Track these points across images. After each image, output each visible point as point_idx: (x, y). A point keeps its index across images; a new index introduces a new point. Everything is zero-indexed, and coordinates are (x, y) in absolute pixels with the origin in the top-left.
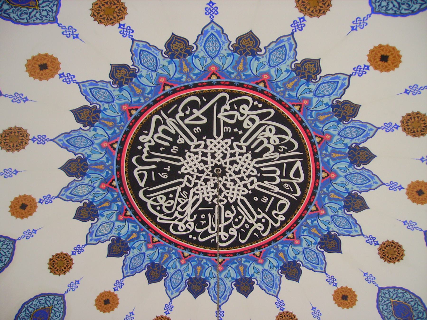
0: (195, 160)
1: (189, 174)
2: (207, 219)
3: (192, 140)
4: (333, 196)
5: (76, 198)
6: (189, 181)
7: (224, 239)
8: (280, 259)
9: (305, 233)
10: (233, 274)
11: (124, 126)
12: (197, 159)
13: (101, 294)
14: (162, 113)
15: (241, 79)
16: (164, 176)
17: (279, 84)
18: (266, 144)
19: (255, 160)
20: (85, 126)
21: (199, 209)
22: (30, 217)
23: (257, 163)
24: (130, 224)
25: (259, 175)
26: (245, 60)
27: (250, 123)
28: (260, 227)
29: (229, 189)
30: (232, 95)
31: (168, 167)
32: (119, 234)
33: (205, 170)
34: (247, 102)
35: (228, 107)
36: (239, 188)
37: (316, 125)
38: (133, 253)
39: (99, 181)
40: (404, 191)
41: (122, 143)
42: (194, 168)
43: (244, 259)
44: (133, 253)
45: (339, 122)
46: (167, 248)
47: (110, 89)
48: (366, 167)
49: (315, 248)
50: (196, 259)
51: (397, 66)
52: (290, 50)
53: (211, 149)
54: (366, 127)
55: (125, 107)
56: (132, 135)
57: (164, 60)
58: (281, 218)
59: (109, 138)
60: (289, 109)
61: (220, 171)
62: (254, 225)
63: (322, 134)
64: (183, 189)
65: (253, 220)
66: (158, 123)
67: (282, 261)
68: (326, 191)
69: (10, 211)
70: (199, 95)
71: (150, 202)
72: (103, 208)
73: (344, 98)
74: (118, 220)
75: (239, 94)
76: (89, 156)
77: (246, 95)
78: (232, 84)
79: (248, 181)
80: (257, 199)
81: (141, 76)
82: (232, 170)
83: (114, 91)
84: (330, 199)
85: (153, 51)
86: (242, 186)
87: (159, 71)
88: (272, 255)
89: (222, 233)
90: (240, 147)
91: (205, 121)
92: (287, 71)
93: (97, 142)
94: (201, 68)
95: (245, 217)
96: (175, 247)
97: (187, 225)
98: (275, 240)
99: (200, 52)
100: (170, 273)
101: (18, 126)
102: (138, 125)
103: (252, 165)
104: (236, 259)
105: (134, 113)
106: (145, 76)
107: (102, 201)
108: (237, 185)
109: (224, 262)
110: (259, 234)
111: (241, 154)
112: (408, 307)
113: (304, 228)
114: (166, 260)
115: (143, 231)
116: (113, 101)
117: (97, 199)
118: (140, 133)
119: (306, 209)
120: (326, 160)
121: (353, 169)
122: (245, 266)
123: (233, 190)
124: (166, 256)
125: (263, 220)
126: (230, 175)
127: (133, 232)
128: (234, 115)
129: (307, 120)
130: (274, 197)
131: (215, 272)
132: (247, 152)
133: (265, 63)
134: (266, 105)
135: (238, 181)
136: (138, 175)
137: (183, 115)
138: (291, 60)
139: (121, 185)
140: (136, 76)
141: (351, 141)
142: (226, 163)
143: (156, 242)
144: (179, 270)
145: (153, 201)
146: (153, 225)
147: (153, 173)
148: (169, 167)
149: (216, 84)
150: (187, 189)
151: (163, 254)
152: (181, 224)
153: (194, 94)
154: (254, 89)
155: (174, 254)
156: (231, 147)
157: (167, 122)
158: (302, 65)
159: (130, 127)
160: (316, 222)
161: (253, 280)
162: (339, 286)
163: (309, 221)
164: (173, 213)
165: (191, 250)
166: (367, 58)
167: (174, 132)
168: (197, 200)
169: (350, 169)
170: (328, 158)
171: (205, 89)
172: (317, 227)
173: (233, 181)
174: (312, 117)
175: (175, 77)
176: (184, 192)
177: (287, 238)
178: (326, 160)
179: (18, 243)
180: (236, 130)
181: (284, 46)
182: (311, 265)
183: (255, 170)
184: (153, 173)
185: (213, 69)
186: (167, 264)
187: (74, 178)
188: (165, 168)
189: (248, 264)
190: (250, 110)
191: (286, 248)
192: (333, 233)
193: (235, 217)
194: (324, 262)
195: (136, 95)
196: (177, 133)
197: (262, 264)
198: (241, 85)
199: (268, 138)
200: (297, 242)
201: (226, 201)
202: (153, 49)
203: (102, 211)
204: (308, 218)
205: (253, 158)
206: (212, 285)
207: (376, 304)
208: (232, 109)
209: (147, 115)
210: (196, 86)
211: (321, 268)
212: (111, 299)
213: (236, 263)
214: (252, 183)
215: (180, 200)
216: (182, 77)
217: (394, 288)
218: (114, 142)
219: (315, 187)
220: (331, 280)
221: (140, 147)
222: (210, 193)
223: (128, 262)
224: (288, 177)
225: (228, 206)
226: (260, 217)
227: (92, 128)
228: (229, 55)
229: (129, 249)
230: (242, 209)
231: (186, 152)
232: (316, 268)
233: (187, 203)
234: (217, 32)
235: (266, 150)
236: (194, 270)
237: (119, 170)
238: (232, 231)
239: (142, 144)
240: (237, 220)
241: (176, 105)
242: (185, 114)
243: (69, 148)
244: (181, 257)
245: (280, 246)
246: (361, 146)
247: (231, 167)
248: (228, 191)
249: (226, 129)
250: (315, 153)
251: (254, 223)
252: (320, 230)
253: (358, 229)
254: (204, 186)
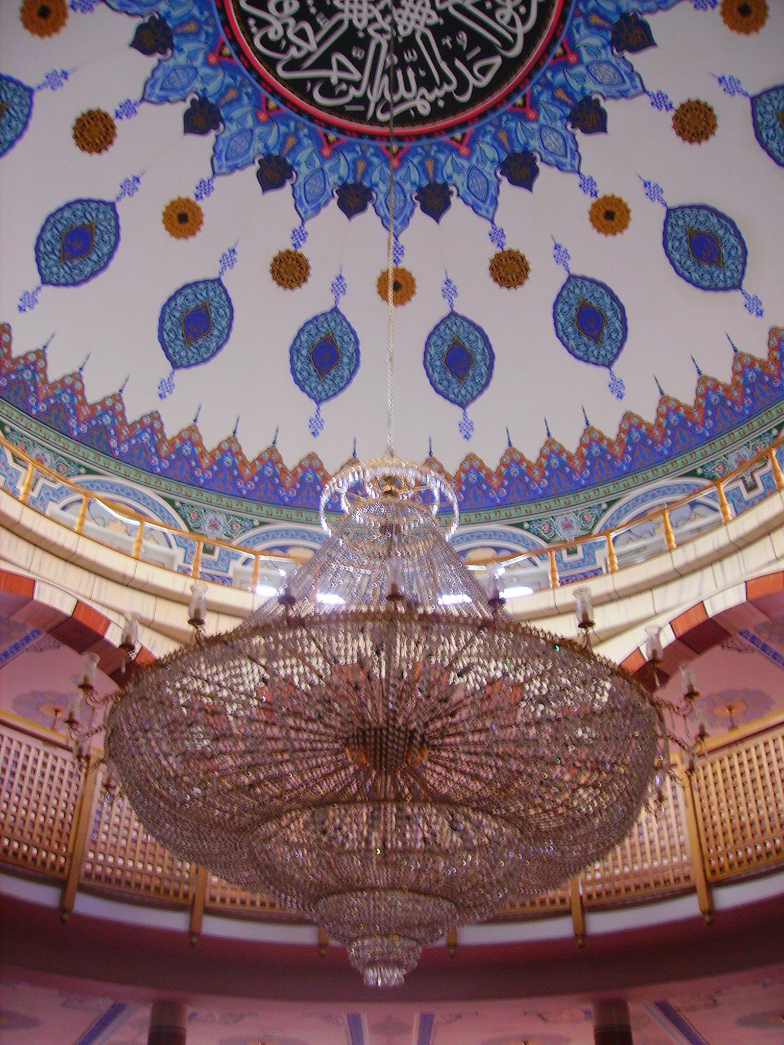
3: (379, 46)
5: (570, 144)
20: (451, 193)
24: (577, 36)
30: (271, 64)
31: (446, 45)
34: (265, 40)
35: (293, 52)
41: (449, 129)
47: (381, 197)
56: (429, 127)
71: (521, 30)
72: (570, 95)
75: (264, 59)
76: (493, 162)
81: (340, 178)
85: (300, 192)
91: (338, 57)
93: (466, 164)
94: (275, 129)
117: (559, 113)
118: (420, 119)
127: (589, 26)
139: (517, 90)
153: (312, 102)
154: (240, 52)
159: (418, 137)
167: (386, 79)
181: (162, 89)
184: (468, 58)
187: (538, 163)
196: (385, 71)
208: (290, 43)
209: (386, 130)
210: (300, 111)
218: (454, 143)
221: (441, 103)
234: (219, 159)
237: (493, 108)
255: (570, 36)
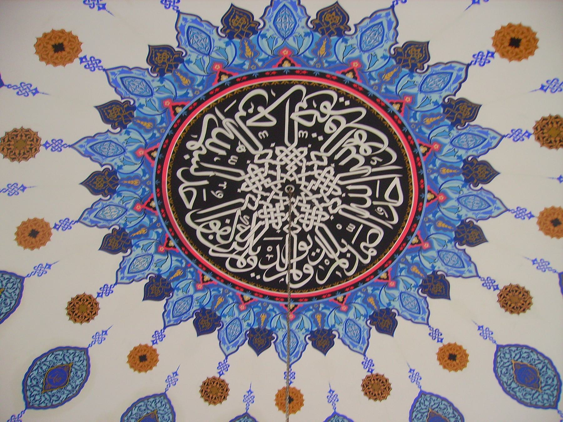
0: (260, 174)
1: (251, 192)
2: (274, 252)
3: (256, 148)
4: (440, 224)
5: (102, 223)
6: (252, 202)
7: (296, 278)
8: (369, 305)
9: (403, 273)
10: (307, 324)
11: (166, 128)
12: (263, 172)
13: (135, 349)
14: (217, 111)
15: (322, 67)
16: (219, 195)
17: (373, 74)
18: (354, 155)
19: (339, 176)
20: (114, 127)
21: (265, 239)
22: (42, 248)
23: (342, 179)
24: (174, 258)
25: (344, 195)
26: (329, 42)
27: (334, 127)
28: (345, 264)
29: (304, 213)
30: (311, 88)
32: (159, 270)
33: (273, 187)
34: (330, 98)
35: (304, 104)
36: (317, 212)
37: (420, 131)
38: (177, 295)
39: (133, 201)
40: (534, 220)
41: (164, 151)
42: (259, 185)
43: (322, 306)
44: (177, 295)
45: (451, 127)
46: (221, 290)
47: (148, 78)
48: (486, 187)
49: (416, 292)
50: (260, 304)
51: (532, 53)
52: (389, 29)
53: (281, 160)
54: (487, 134)
55: (168, 103)
56: (176, 141)
57: (220, 40)
58: (372, 252)
59: (146, 144)
60: (385, 108)
61: (292, 190)
62: (336, 261)
63: (428, 143)
64: (243, 213)
65: (334, 253)
66: (212, 125)
67: (372, 308)
68: (432, 218)
69: (16, 239)
70: (267, 88)
71: (199, 229)
72: (139, 237)
73: (459, 95)
74: (157, 252)
76: (120, 167)
77: (328, 88)
78: (310, 74)
79: (329, 203)
80: (341, 228)
81: (189, 62)
82: (309, 188)
83: (153, 81)
84: (436, 228)
85: (205, 28)
86: (321, 209)
87: (214, 55)
88: (359, 300)
89: (294, 271)
90: (319, 158)
92: (384, 57)
93: (130, 149)
94: (269, 52)
95: (325, 250)
96: (232, 289)
97: (249, 259)
98: (363, 281)
99: (268, 30)
100: (226, 322)
101: (26, 127)
102: (185, 126)
103: (335, 182)
104: (313, 305)
105: (179, 110)
106: (194, 61)
107: (137, 226)
108: (315, 208)
109: (295, 309)
110: (343, 273)
111: (321, 168)
112: (534, 371)
113: (402, 266)
114: (221, 306)
115: (190, 267)
116: (152, 95)
117: (130, 225)
118: (187, 137)
119: (406, 241)
120: (432, 176)
121: (468, 190)
122: (324, 315)
123: (310, 214)
124: (220, 300)
125: (348, 255)
126: (306, 195)
127: (177, 268)
128: (313, 115)
129: (410, 124)
130: (364, 225)
131: (284, 322)
132: (329, 165)
133: (355, 46)
134: (355, 103)
135: (316, 202)
136: (185, 193)
137: (244, 114)
138: (390, 43)
139: (162, 206)
140: (182, 61)
141: (467, 152)
142: (300, 179)
143: (207, 281)
144: (237, 318)
145: (203, 227)
146: (203, 259)
147: (204, 191)
148: (225, 183)
149: (289, 74)
150: (248, 212)
151: (216, 297)
152: (241, 259)
153: (260, 87)
154: (340, 81)
155: (232, 297)
156: (308, 158)
157: (224, 123)
158: (404, 50)
159: (175, 130)
160: (417, 259)
161: (334, 332)
162: (445, 342)
163: (409, 258)
164: (231, 244)
165: (253, 293)
166: (491, 42)
167: (232, 137)
168: (262, 227)
169: (464, 189)
170: (435, 175)
171: (275, 80)
172: (419, 265)
173: (309, 202)
174: (415, 119)
175: (234, 63)
176: (244, 217)
177: (379, 278)
178: (432, 176)
179: (26, 282)
180: (314, 135)
181: (381, 23)
182: (410, 315)
183: (339, 190)
184: (204, 191)
185: (285, 53)
186: (221, 310)
187: (100, 196)
188: (220, 185)
189: (327, 312)
190: (333, 109)
191: (378, 292)
192: (439, 273)
193: (311, 251)
194: (427, 310)
195: (182, 87)
197: (346, 312)
198: (322, 76)
199: (358, 147)
200: (392, 284)
201: (300, 229)
202: (205, 26)
203: (136, 240)
204: (407, 253)
205: (337, 172)
206: (281, 338)
207: (492, 366)
208: (310, 107)
209: (197, 114)
210: (262, 75)
211: (423, 319)
212: (148, 355)
213: (312, 310)
214: (335, 206)
215: (239, 227)
216: (244, 64)
217: (517, 346)
218: (153, 148)
219: (418, 213)
220: (436, 335)
221: (187, 157)
222: (279, 218)
223: (170, 307)
224: (382, 198)
225: (302, 236)
226: (344, 250)
227: (124, 131)
228: (307, 35)
229: (172, 290)
230: (321, 240)
231: (248, 164)
232: (416, 318)
233: (248, 231)
235: (354, 162)
236: (256, 318)
237: (159, 186)
238: (306, 269)
239: (191, 153)
240: (313, 254)
241: (235, 101)
242: (247, 113)
243: (93, 157)
244: (240, 301)
245: (370, 290)
246: (480, 159)
247: (307, 184)
248: (302, 216)
249: (301, 134)
250: (419, 168)
251: (337, 259)
252: (422, 269)
253: (472, 268)
254: (271, 209)
255: (178, 255)
